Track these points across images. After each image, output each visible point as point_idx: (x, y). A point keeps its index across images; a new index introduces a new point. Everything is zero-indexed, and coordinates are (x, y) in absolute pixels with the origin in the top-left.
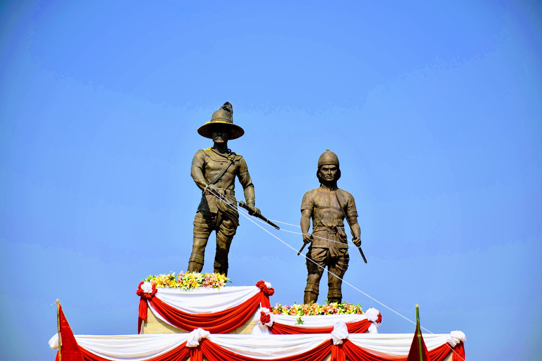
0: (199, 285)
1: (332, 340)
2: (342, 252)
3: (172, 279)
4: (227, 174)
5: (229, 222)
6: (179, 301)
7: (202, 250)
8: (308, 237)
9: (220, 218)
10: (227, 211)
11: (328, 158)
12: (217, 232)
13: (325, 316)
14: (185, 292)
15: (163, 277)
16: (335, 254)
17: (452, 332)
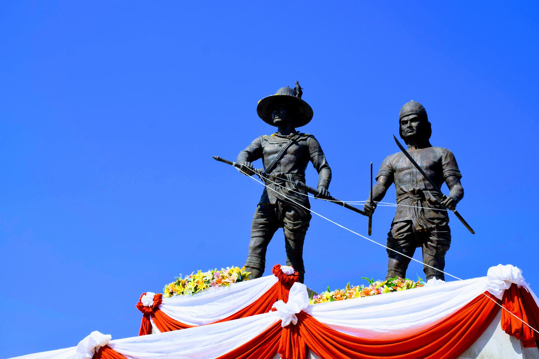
2: (433, 223)
4: (288, 156)
5: (292, 213)
8: (368, 205)
9: (281, 209)
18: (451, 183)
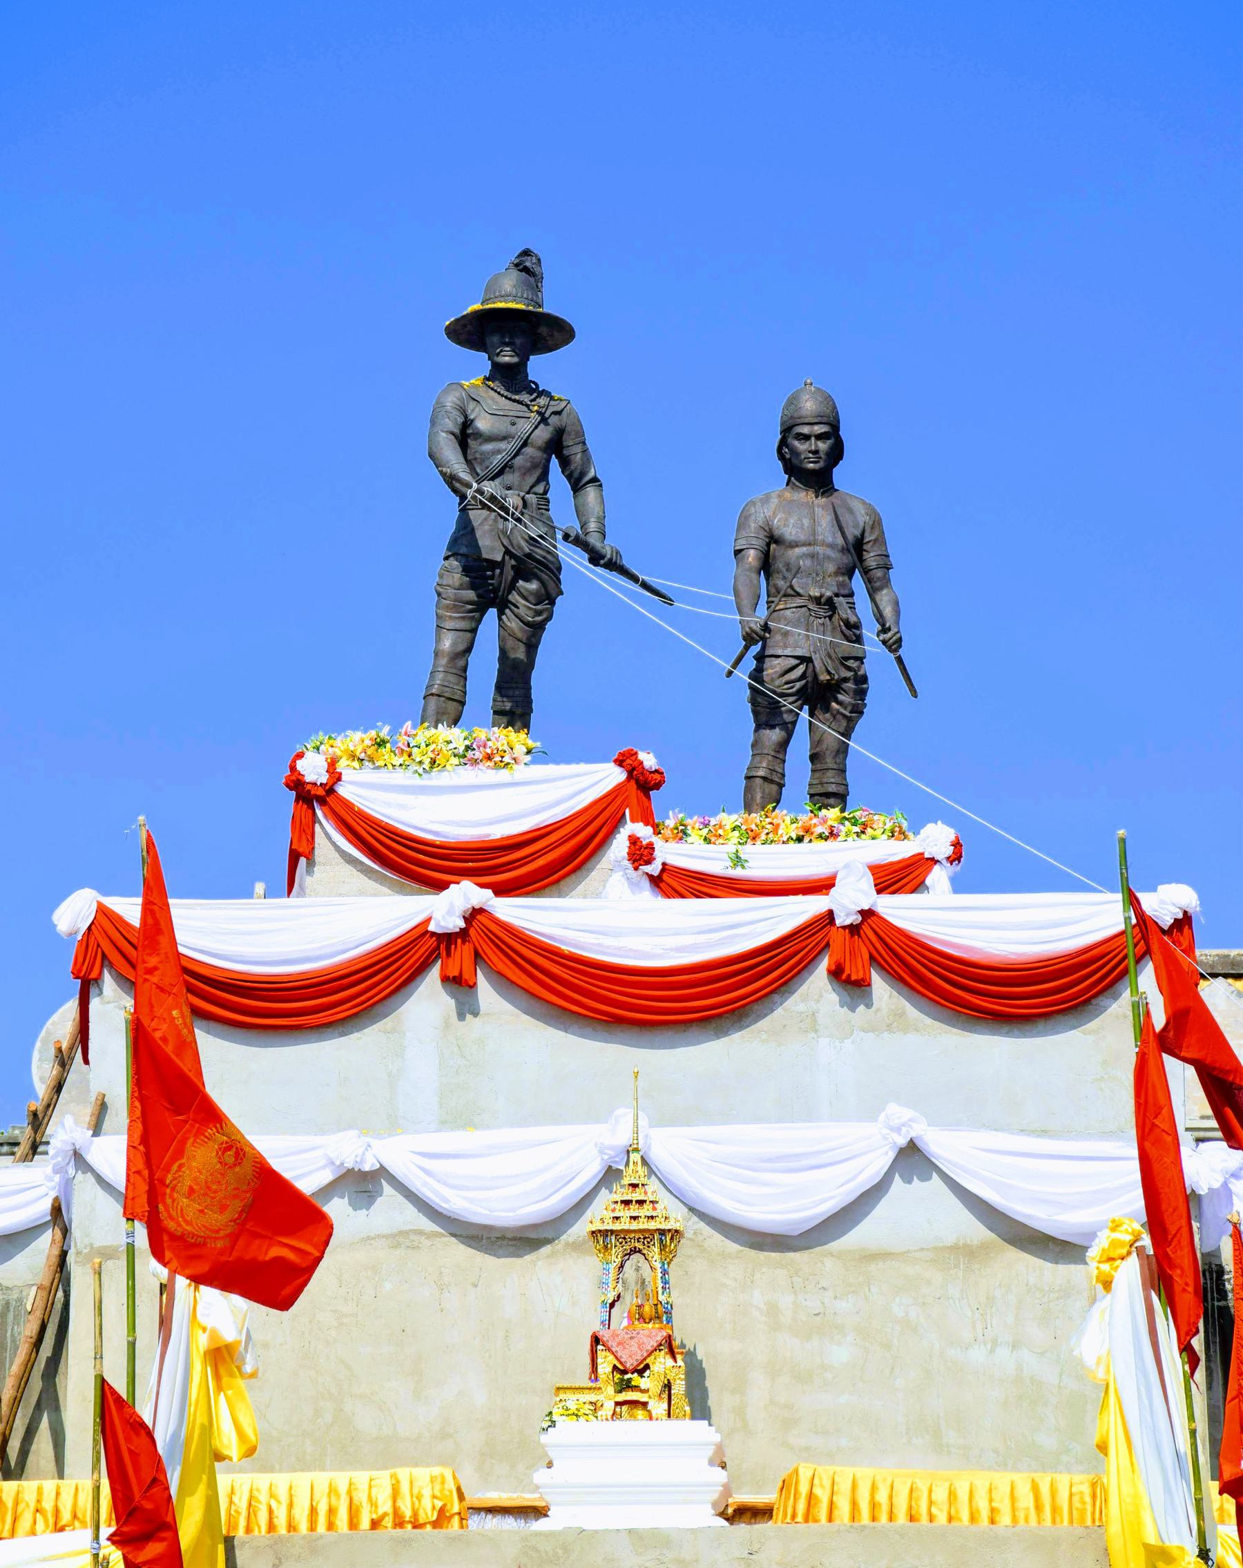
0: (455, 761)
1: (830, 914)
2: (849, 669)
3: (381, 743)
4: (528, 450)
5: (533, 586)
6: (402, 807)
7: (461, 663)
8: (757, 628)
9: (509, 573)
10: (529, 556)
11: (809, 406)
12: (501, 613)
13: (804, 846)
14: (418, 781)
15: (356, 740)
16: (829, 673)
17: (1162, 888)
18: (878, 584)
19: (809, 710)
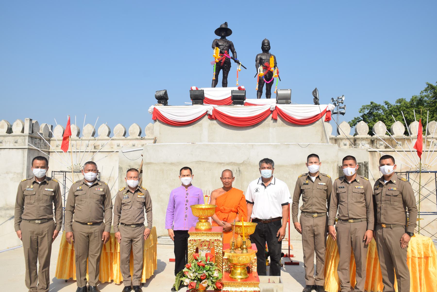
19: (266, 84)
